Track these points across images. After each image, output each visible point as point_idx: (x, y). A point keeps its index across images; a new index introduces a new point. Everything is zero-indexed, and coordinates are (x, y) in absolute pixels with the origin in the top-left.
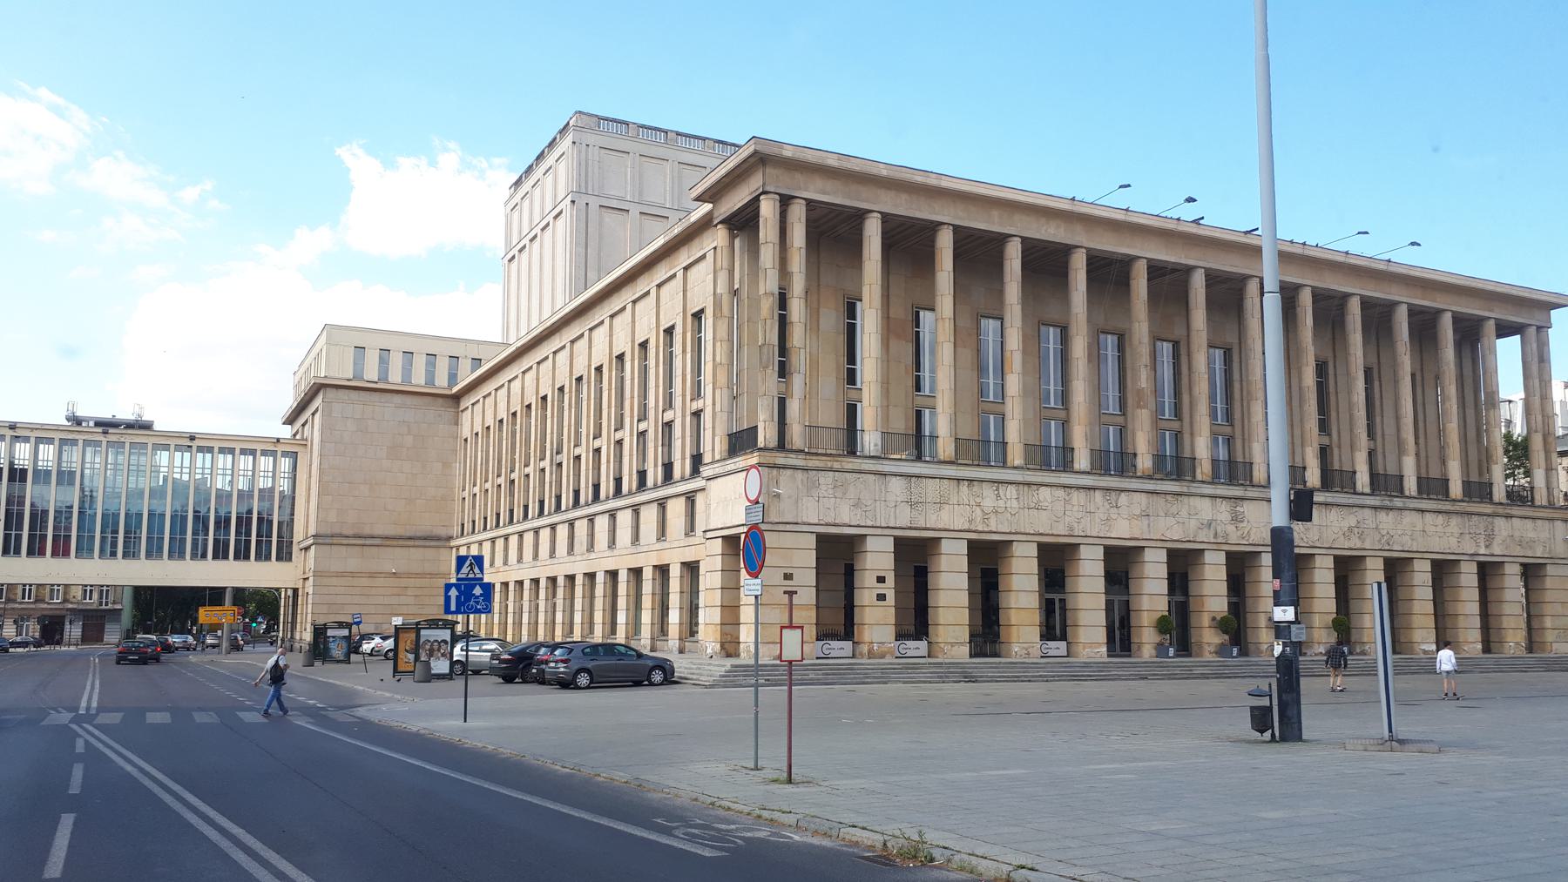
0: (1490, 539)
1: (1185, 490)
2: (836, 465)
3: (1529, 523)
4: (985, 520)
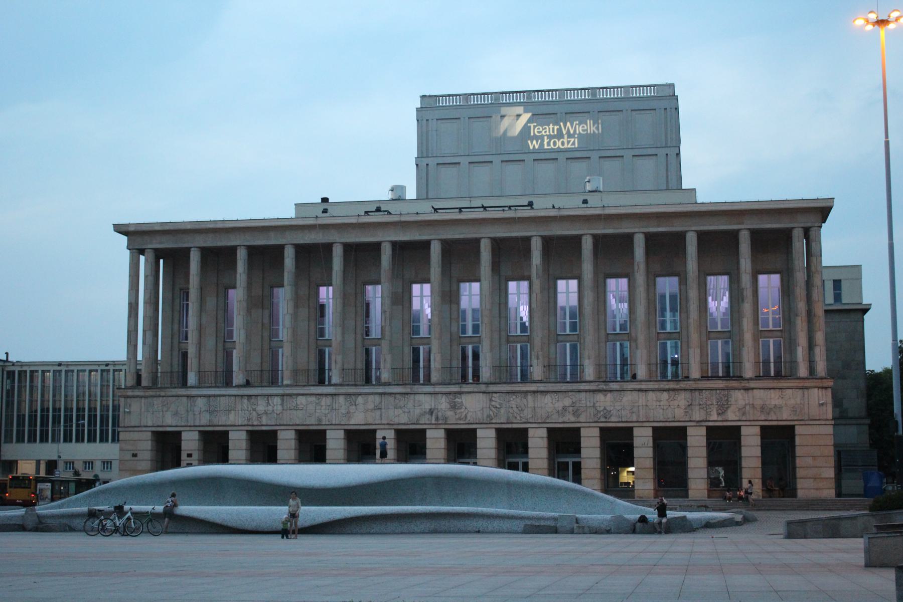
0: (723, 409)
1: (408, 390)
2: (162, 393)
3: (773, 394)
4: (259, 416)
